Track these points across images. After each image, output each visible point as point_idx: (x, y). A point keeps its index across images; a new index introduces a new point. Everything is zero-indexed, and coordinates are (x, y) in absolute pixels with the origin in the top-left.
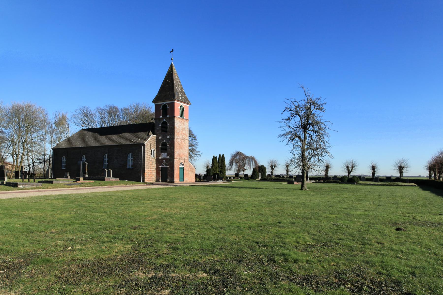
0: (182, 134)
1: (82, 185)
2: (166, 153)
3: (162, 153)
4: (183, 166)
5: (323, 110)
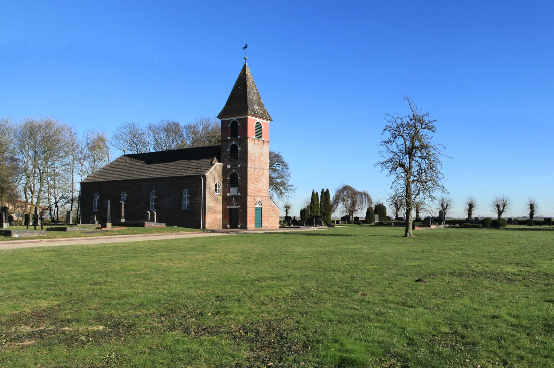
0: (260, 162)
1: (107, 233)
2: (236, 188)
3: (231, 189)
4: (261, 206)
5: (433, 130)
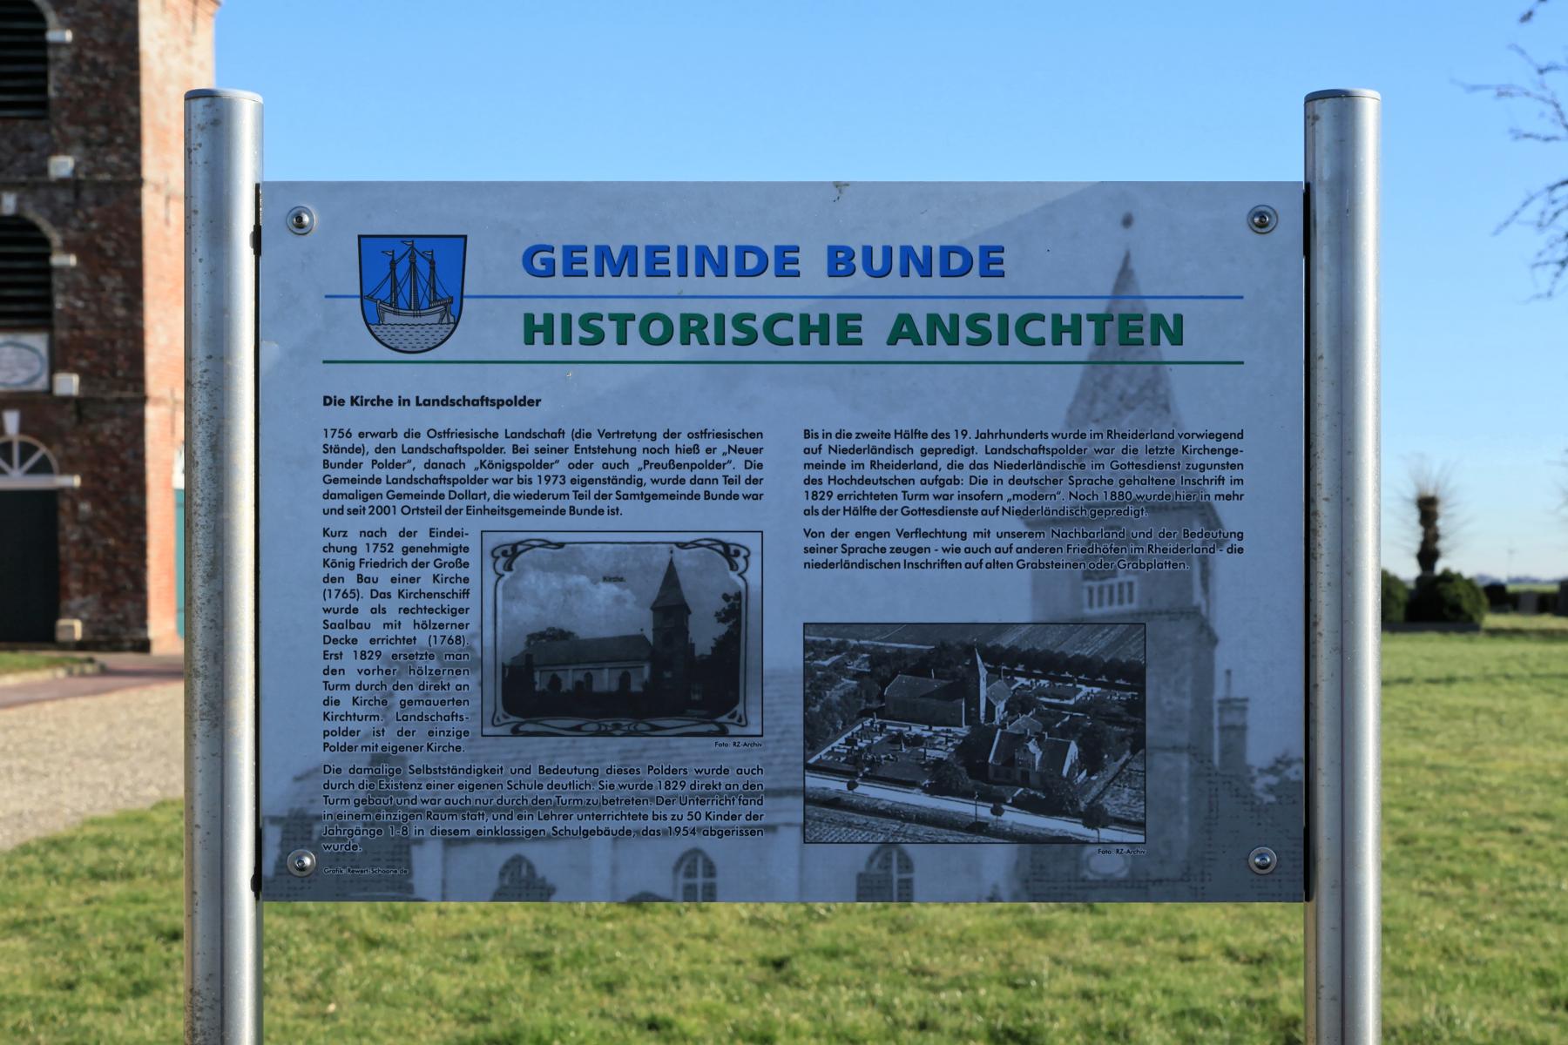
2: (38, 342)
